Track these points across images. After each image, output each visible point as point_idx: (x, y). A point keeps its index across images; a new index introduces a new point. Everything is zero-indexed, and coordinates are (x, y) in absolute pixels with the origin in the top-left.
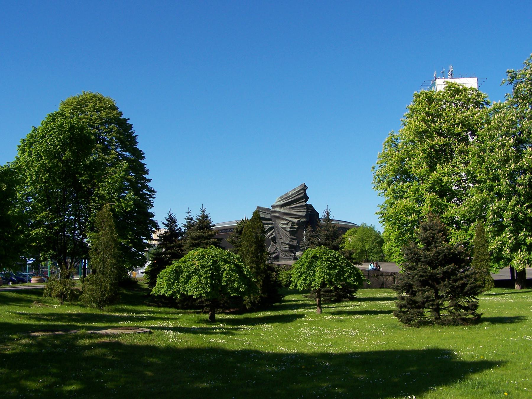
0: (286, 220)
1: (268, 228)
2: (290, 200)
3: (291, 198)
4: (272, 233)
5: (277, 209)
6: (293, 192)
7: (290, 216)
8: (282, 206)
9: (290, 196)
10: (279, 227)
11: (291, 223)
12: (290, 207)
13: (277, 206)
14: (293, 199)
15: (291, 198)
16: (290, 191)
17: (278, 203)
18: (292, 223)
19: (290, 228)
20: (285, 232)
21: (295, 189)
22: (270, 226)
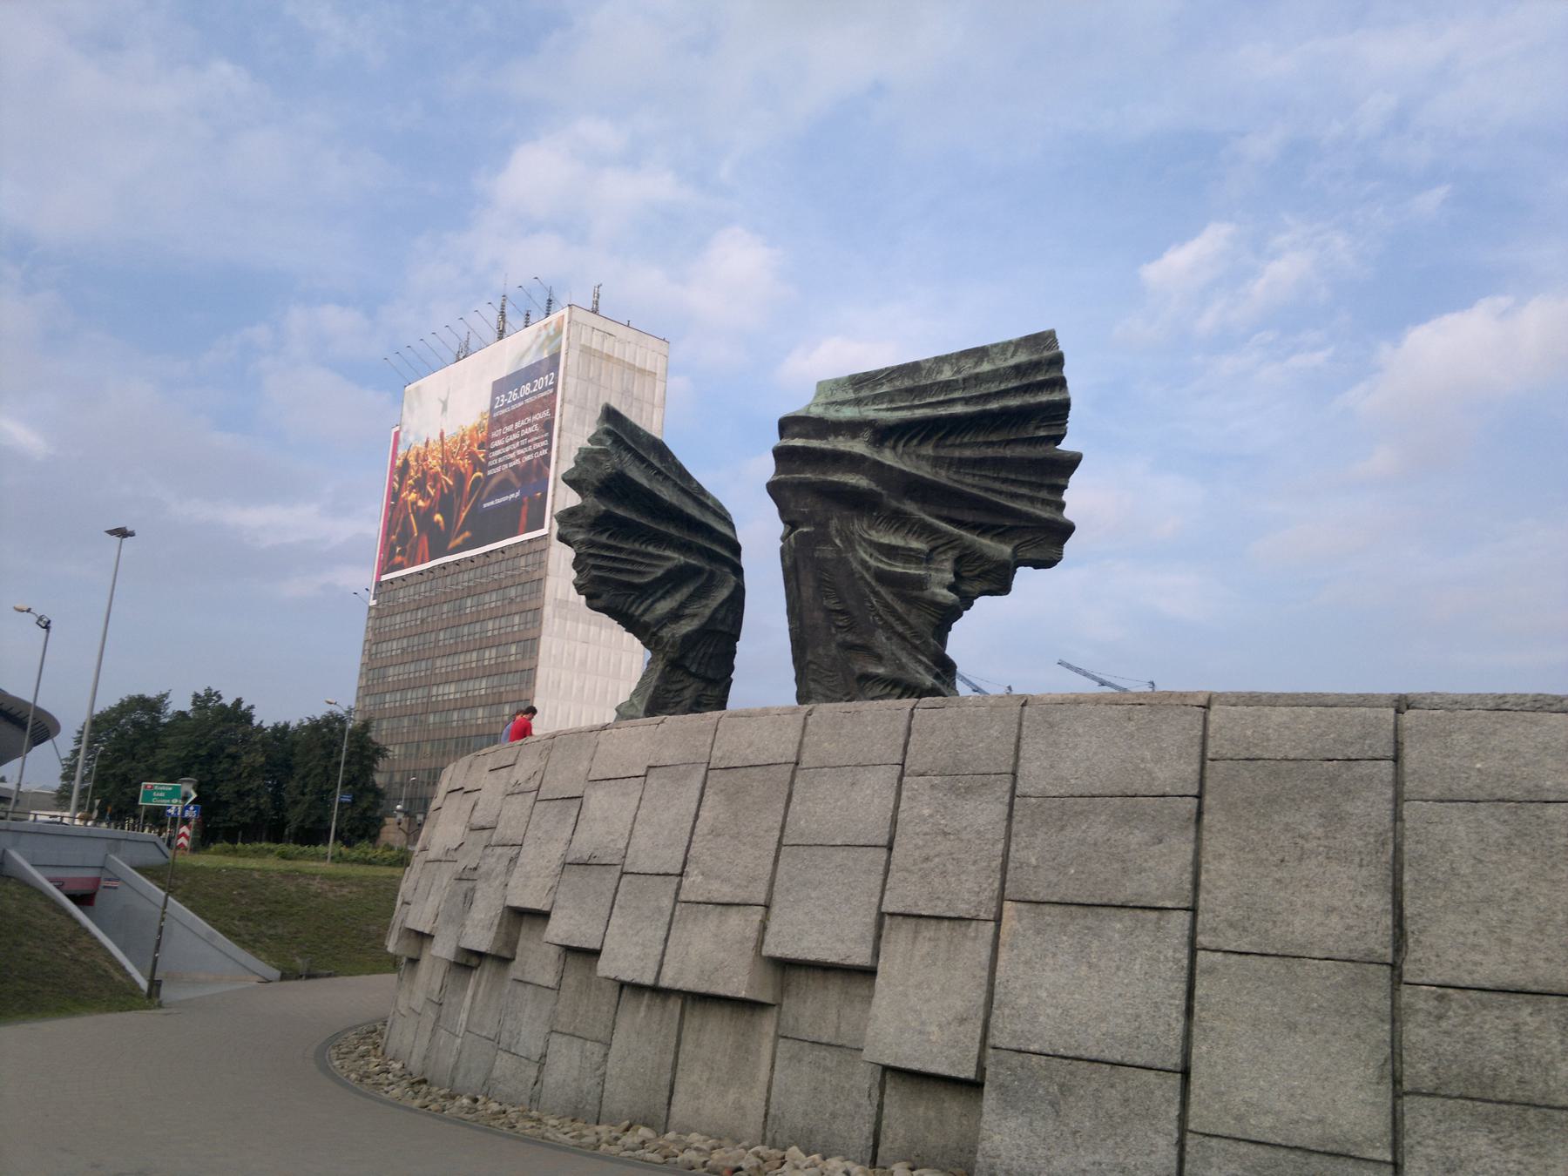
0: (924, 530)
1: (669, 565)
2: (959, 409)
3: (967, 401)
4: (683, 605)
5: (859, 447)
6: (969, 368)
7: (945, 512)
8: (884, 434)
9: (948, 386)
10: (855, 565)
11: (951, 554)
12: (943, 452)
13: (852, 428)
14: (994, 406)
15: (967, 401)
16: (940, 361)
17: (848, 413)
18: (958, 561)
19: (952, 588)
20: (900, 607)
21: (981, 353)
22: (678, 558)
